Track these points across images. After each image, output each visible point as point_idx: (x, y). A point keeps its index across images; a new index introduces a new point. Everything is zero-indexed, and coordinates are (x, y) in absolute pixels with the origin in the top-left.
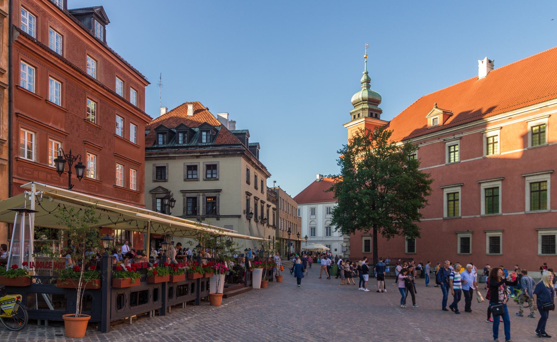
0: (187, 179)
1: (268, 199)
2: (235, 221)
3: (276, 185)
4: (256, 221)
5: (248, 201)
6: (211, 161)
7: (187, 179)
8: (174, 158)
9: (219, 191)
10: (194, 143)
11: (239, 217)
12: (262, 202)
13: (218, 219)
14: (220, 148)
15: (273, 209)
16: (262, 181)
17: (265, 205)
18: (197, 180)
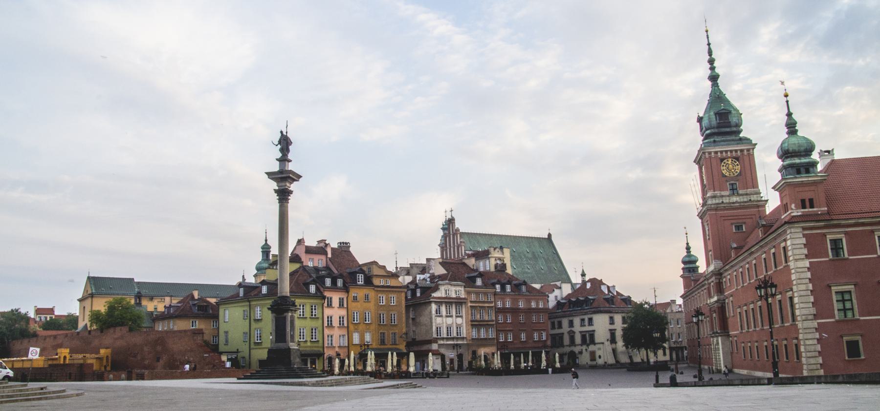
0: (582, 326)
2: (601, 346)
6: (590, 316)
7: (582, 326)
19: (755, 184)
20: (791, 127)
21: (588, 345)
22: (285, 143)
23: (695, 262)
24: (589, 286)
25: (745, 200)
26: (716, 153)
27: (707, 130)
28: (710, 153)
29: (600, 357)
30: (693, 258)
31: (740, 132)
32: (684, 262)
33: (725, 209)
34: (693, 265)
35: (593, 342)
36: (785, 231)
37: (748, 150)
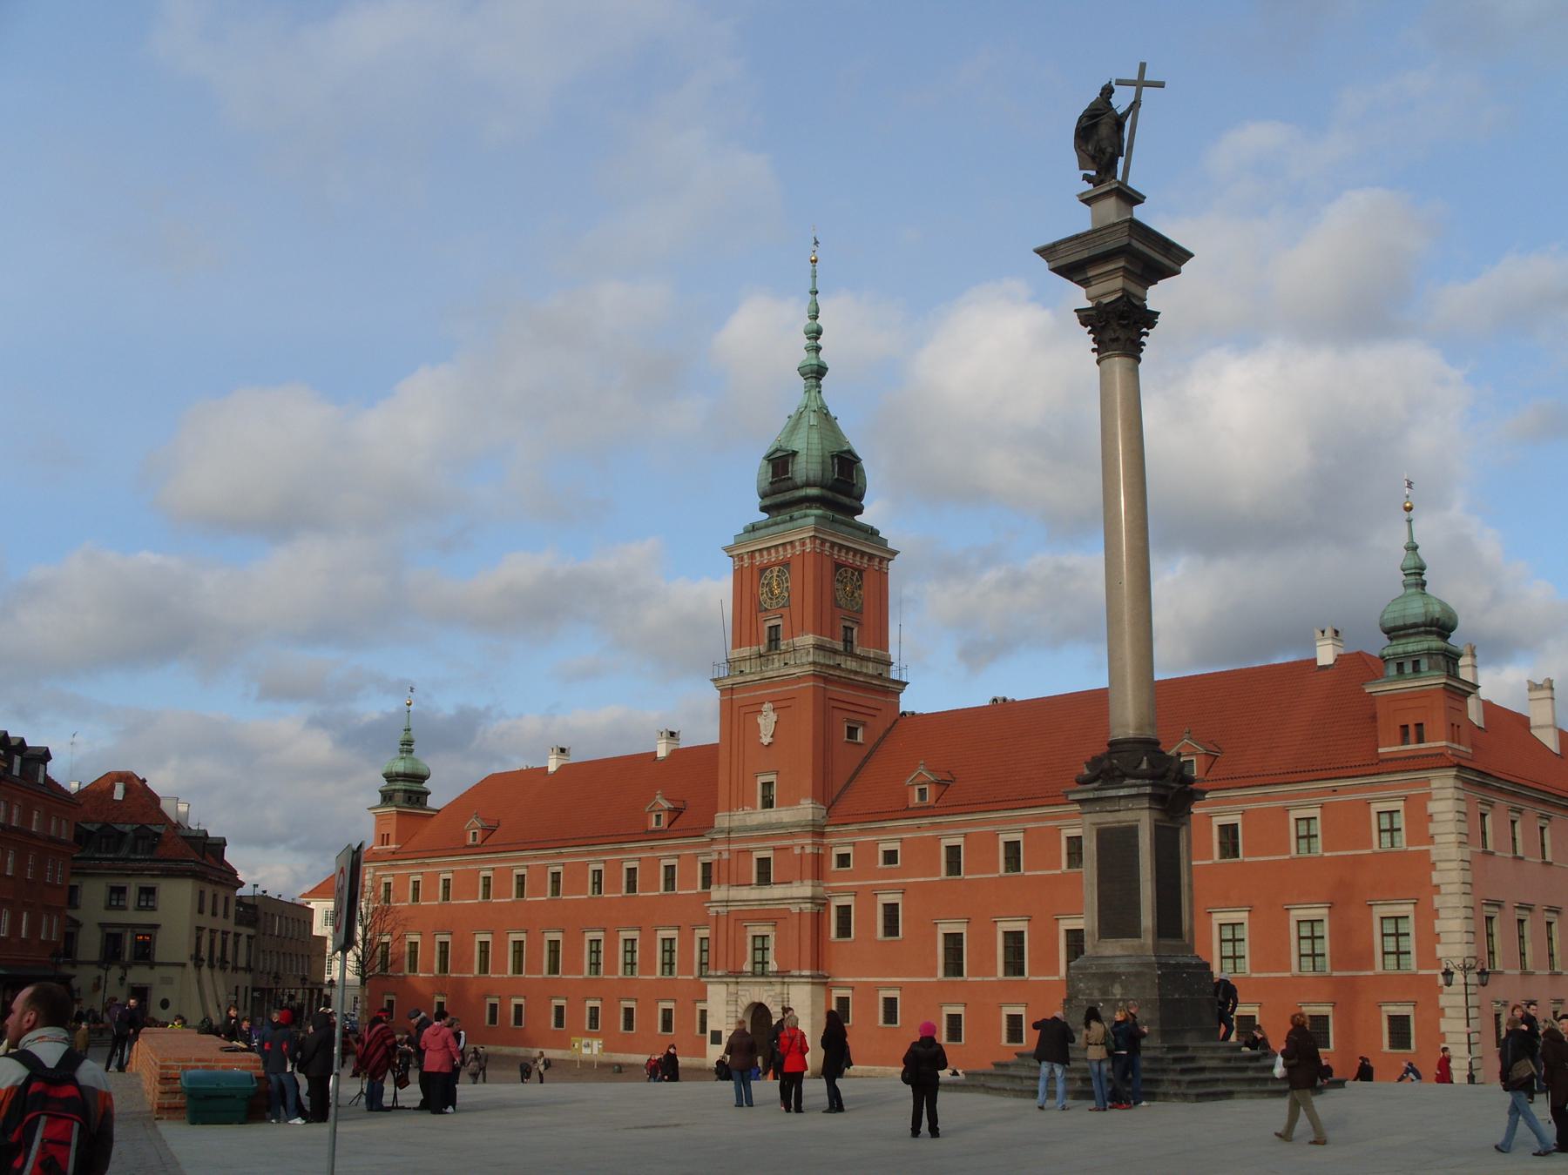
0: (109, 907)
1: (239, 921)
3: (259, 891)
4: (211, 966)
5: (199, 939)
6: (148, 882)
8: (92, 875)
9: (156, 927)
10: (122, 854)
11: (184, 965)
12: (225, 933)
13: (152, 968)
14: (161, 865)
15: (249, 937)
16: (227, 899)
17: (231, 936)
18: (124, 908)
19: (883, 643)
20: (1416, 575)
21: (126, 967)
22: (1101, 137)
23: (422, 778)
24: (119, 792)
25: (871, 671)
26: (833, 544)
27: (808, 484)
28: (823, 542)
29: (165, 1004)
30: (422, 770)
31: (860, 511)
32: (390, 777)
33: (839, 681)
34: (415, 787)
35: (144, 954)
36: (1427, 781)
37: (882, 560)
